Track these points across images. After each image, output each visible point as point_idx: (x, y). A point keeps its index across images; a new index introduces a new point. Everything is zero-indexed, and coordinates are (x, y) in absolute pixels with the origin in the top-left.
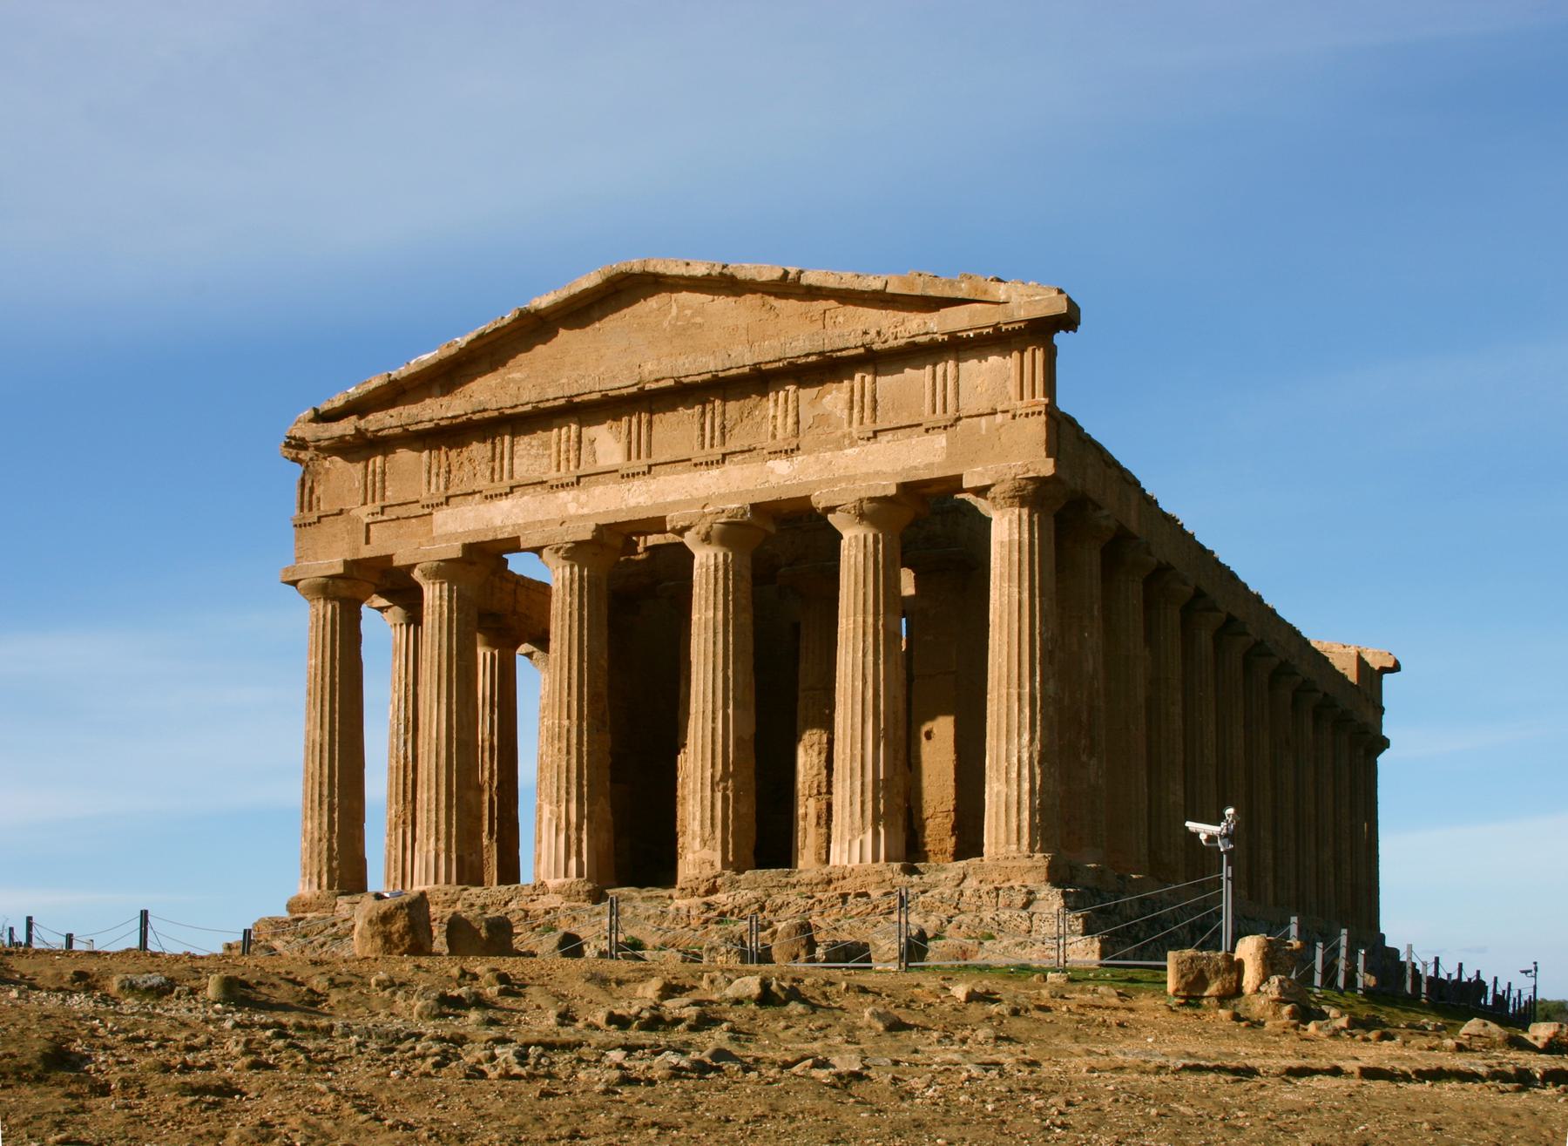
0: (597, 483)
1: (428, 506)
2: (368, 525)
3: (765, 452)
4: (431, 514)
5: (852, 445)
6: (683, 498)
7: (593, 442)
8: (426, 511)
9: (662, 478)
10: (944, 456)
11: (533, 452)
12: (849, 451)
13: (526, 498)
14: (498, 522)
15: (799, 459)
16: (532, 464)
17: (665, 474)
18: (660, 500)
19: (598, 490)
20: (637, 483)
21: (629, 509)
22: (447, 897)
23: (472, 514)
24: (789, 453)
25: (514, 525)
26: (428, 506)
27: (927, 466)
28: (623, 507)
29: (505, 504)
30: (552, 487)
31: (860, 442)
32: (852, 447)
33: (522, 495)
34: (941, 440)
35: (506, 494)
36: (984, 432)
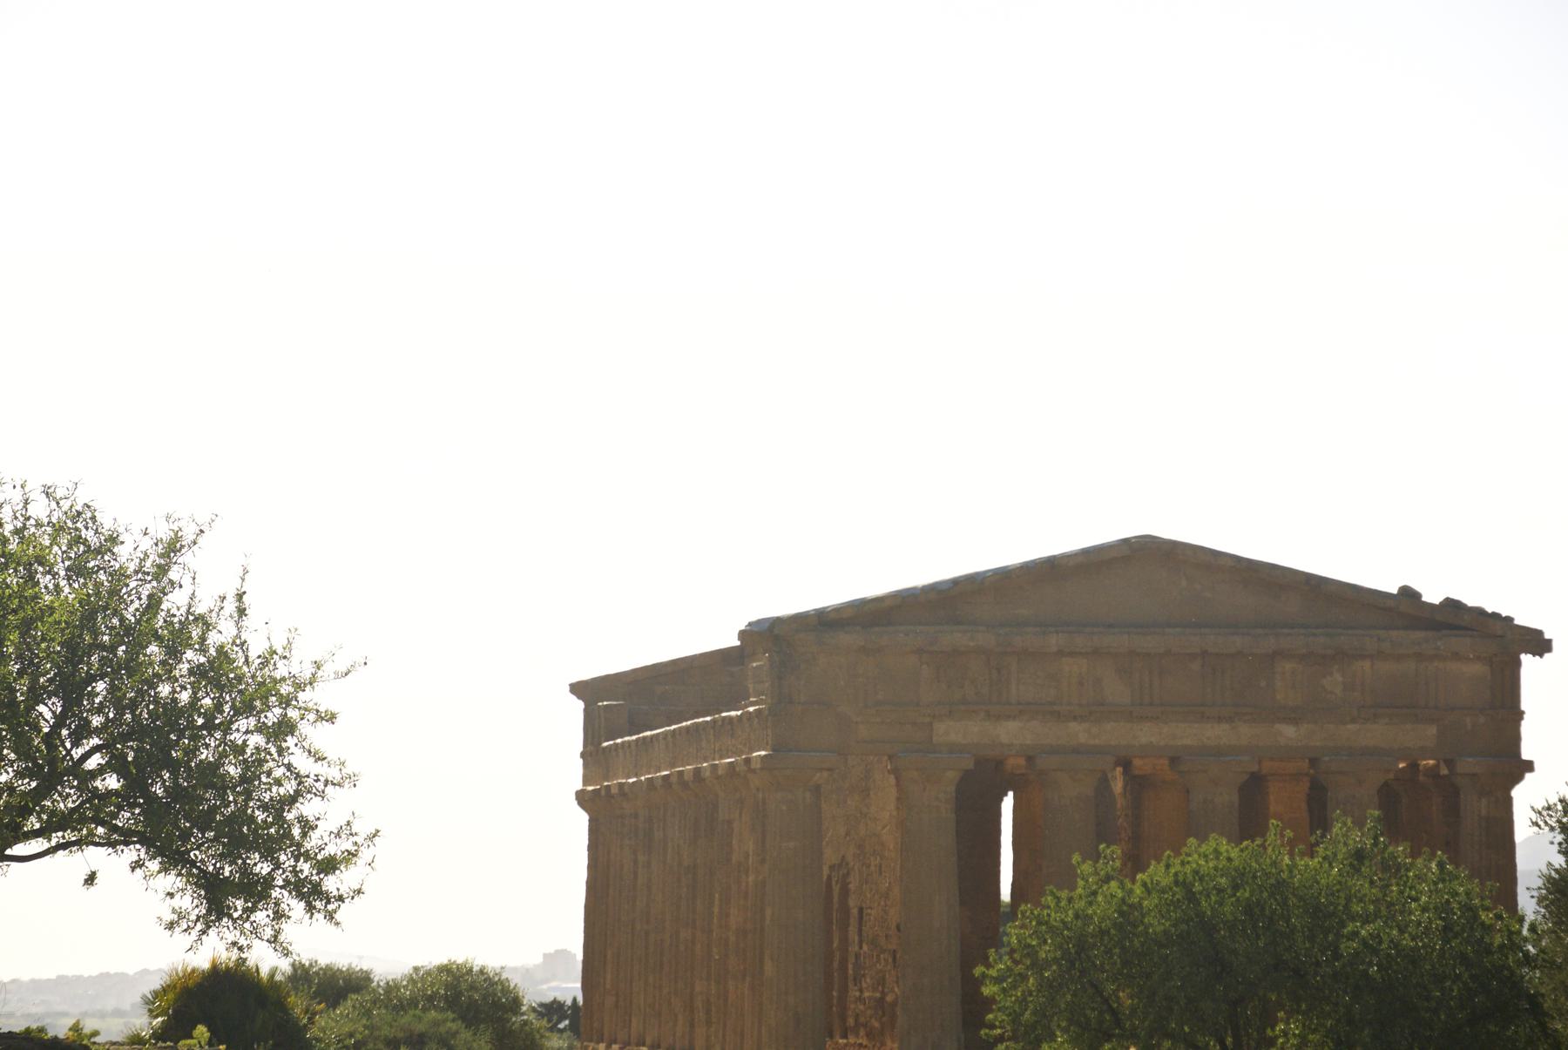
2: (857, 723)
5: (1353, 721)
12: (1349, 726)
14: (1004, 739)
24: (1295, 721)
29: (1013, 725)
34: (1432, 730)
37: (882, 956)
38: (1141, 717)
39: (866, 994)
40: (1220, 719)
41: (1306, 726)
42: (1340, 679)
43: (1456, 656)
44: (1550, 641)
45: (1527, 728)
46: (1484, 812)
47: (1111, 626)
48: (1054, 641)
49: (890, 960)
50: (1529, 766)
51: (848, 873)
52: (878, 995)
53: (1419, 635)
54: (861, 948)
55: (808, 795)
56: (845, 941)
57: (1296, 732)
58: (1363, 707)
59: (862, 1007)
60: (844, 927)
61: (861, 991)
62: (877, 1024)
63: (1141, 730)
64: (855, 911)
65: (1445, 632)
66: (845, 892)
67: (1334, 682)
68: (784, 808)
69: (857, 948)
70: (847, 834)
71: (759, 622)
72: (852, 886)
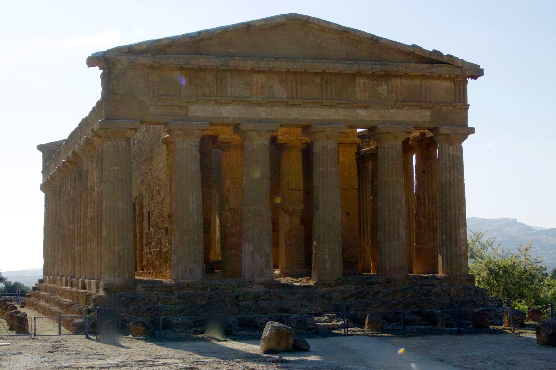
1: (187, 102)
3: (355, 105)
4: (187, 106)
6: (318, 118)
9: (308, 108)
10: (430, 119)
11: (241, 86)
14: (225, 115)
15: (370, 111)
18: (307, 118)
19: (276, 109)
20: (295, 110)
24: (366, 108)
25: (233, 118)
26: (187, 102)
27: (424, 122)
28: (290, 119)
31: (395, 108)
32: (393, 109)
33: (237, 105)
34: (428, 113)
35: (230, 103)
36: (445, 112)
37: (160, 231)
38: (292, 104)
39: (152, 250)
40: (330, 107)
41: (370, 110)
42: (386, 88)
43: (440, 77)
44: (483, 70)
45: (471, 113)
46: (451, 153)
47: (277, 58)
48: (250, 64)
49: (164, 232)
50: (472, 131)
51: (143, 199)
52: (158, 249)
53: (424, 66)
54: (149, 229)
55: (124, 142)
56: (142, 229)
57: (366, 113)
58: (397, 101)
59: (150, 256)
60: (141, 222)
61: (150, 249)
62: (157, 263)
63: (292, 111)
64: (146, 214)
65: (435, 65)
66: (142, 207)
67: (383, 89)
68: (112, 149)
69: (147, 230)
70: (142, 182)
71: (97, 53)
72: (145, 204)
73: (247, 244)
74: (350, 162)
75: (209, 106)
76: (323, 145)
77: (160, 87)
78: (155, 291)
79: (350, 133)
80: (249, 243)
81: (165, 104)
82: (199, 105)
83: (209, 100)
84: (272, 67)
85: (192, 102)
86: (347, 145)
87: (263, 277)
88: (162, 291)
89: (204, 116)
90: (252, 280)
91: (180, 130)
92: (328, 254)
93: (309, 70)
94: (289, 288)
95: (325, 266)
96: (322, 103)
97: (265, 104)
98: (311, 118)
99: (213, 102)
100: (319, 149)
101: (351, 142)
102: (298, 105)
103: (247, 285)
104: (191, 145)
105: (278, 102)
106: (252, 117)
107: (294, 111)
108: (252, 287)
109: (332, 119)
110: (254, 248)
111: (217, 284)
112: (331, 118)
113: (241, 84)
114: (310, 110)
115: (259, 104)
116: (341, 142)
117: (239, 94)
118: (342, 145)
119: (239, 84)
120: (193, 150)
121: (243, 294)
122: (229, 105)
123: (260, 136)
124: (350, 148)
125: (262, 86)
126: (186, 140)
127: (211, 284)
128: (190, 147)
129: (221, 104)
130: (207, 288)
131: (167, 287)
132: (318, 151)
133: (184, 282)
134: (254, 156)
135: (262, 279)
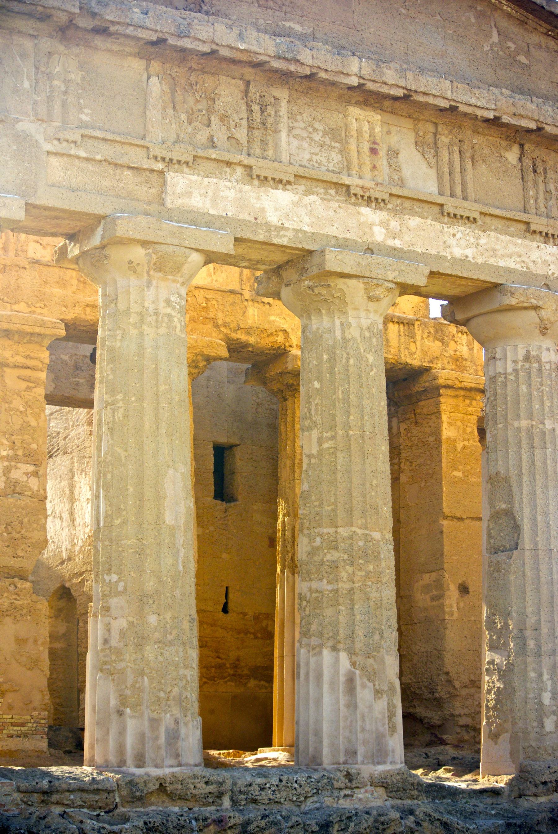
0: (411, 210)
1: (163, 159)
2: (48, 153)
4: (162, 172)
6: (518, 267)
7: (393, 153)
8: (160, 166)
9: (492, 234)
11: (317, 137)
13: (312, 198)
14: (273, 218)
16: (317, 154)
17: (496, 230)
18: (492, 261)
19: (414, 221)
20: (460, 230)
21: (455, 261)
22: (212, 788)
23: (231, 194)
25: (297, 231)
26: (163, 159)
30: (355, 195)
33: (308, 192)
35: (289, 183)
38: (455, 215)
63: (454, 235)
73: (326, 653)
74: (466, 443)
75: (228, 184)
76: (528, 351)
77: (82, 101)
78: (57, 803)
79: (466, 360)
80: (334, 649)
81: (99, 157)
82: (198, 175)
83: (229, 164)
84: (413, 88)
85: (179, 162)
86: (462, 393)
87: (385, 763)
88: (81, 807)
89: (212, 212)
90: (353, 771)
91: (145, 244)
92: (549, 688)
93: (505, 119)
94: (444, 797)
95: (543, 726)
96: (528, 224)
97: (383, 200)
98: (502, 263)
99: (239, 171)
100: (515, 362)
101: (473, 385)
102: (468, 218)
103: (341, 789)
104: (168, 302)
105: (418, 200)
106: (348, 236)
107: (459, 235)
108: (352, 796)
109: (553, 274)
110: (354, 664)
111: (250, 785)
112: (550, 273)
113: (315, 130)
114: (497, 238)
115: (369, 198)
116: (450, 383)
117: (309, 160)
118: (449, 392)
119: (310, 129)
120: (176, 319)
121: (344, 818)
122: (285, 190)
123: (370, 298)
124: (467, 402)
125: (376, 146)
126: (154, 283)
127: (235, 784)
128: (169, 310)
129: (264, 180)
130: (220, 795)
131: (97, 791)
132: (509, 370)
133: (147, 774)
134: (352, 361)
135: (381, 768)
